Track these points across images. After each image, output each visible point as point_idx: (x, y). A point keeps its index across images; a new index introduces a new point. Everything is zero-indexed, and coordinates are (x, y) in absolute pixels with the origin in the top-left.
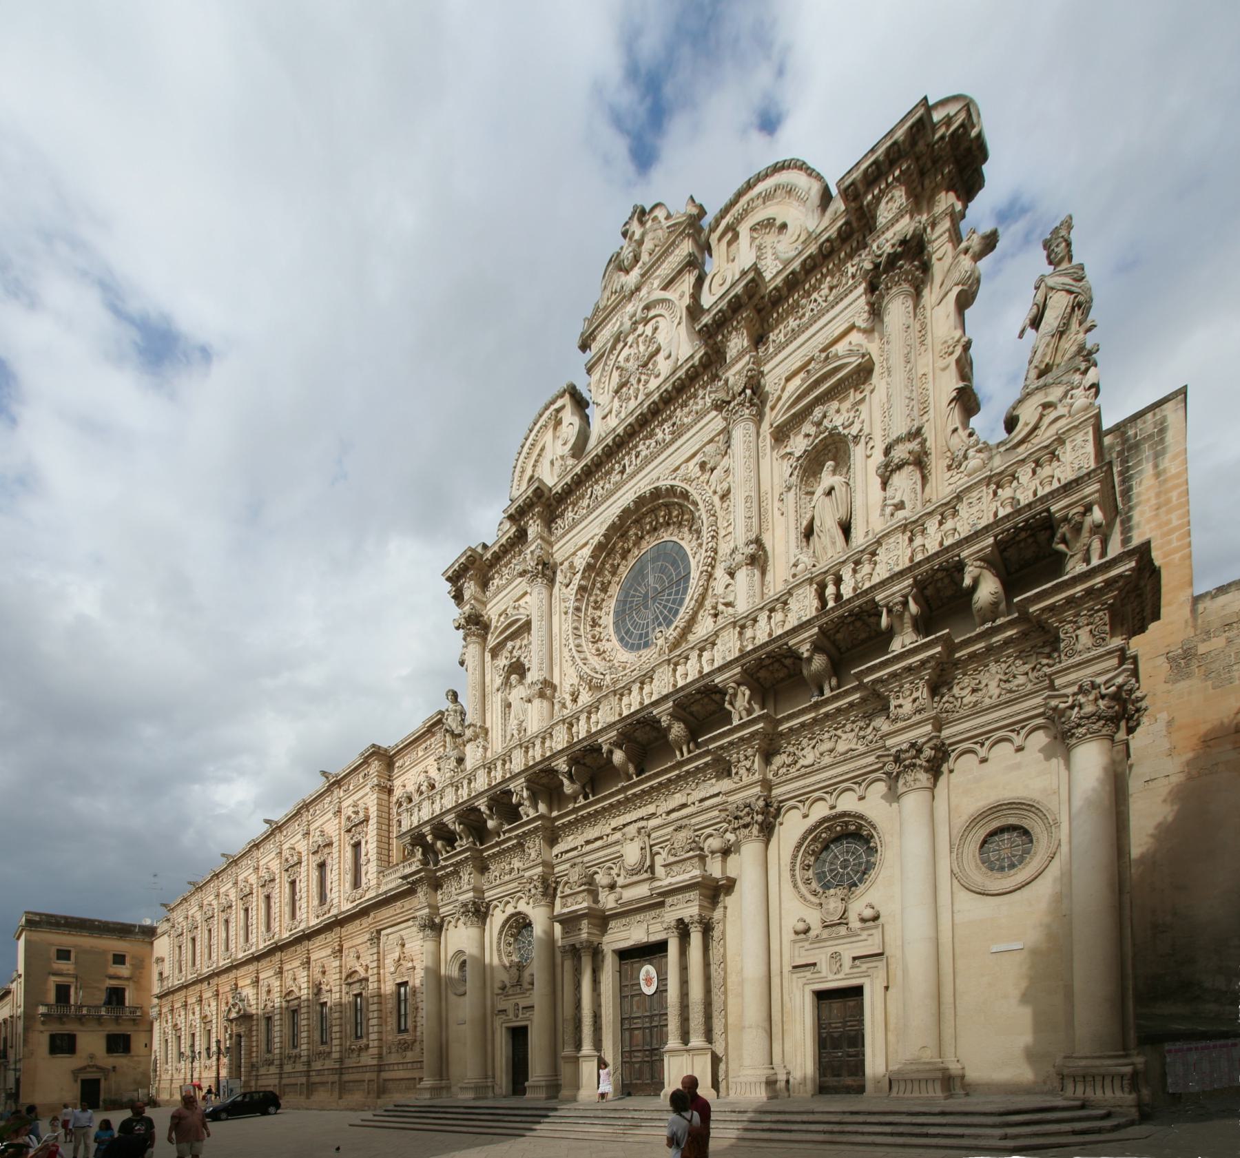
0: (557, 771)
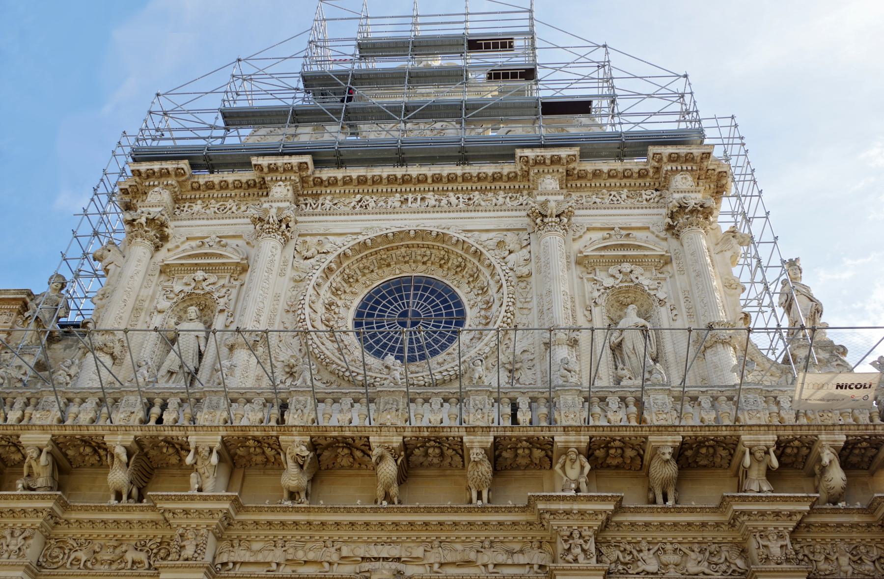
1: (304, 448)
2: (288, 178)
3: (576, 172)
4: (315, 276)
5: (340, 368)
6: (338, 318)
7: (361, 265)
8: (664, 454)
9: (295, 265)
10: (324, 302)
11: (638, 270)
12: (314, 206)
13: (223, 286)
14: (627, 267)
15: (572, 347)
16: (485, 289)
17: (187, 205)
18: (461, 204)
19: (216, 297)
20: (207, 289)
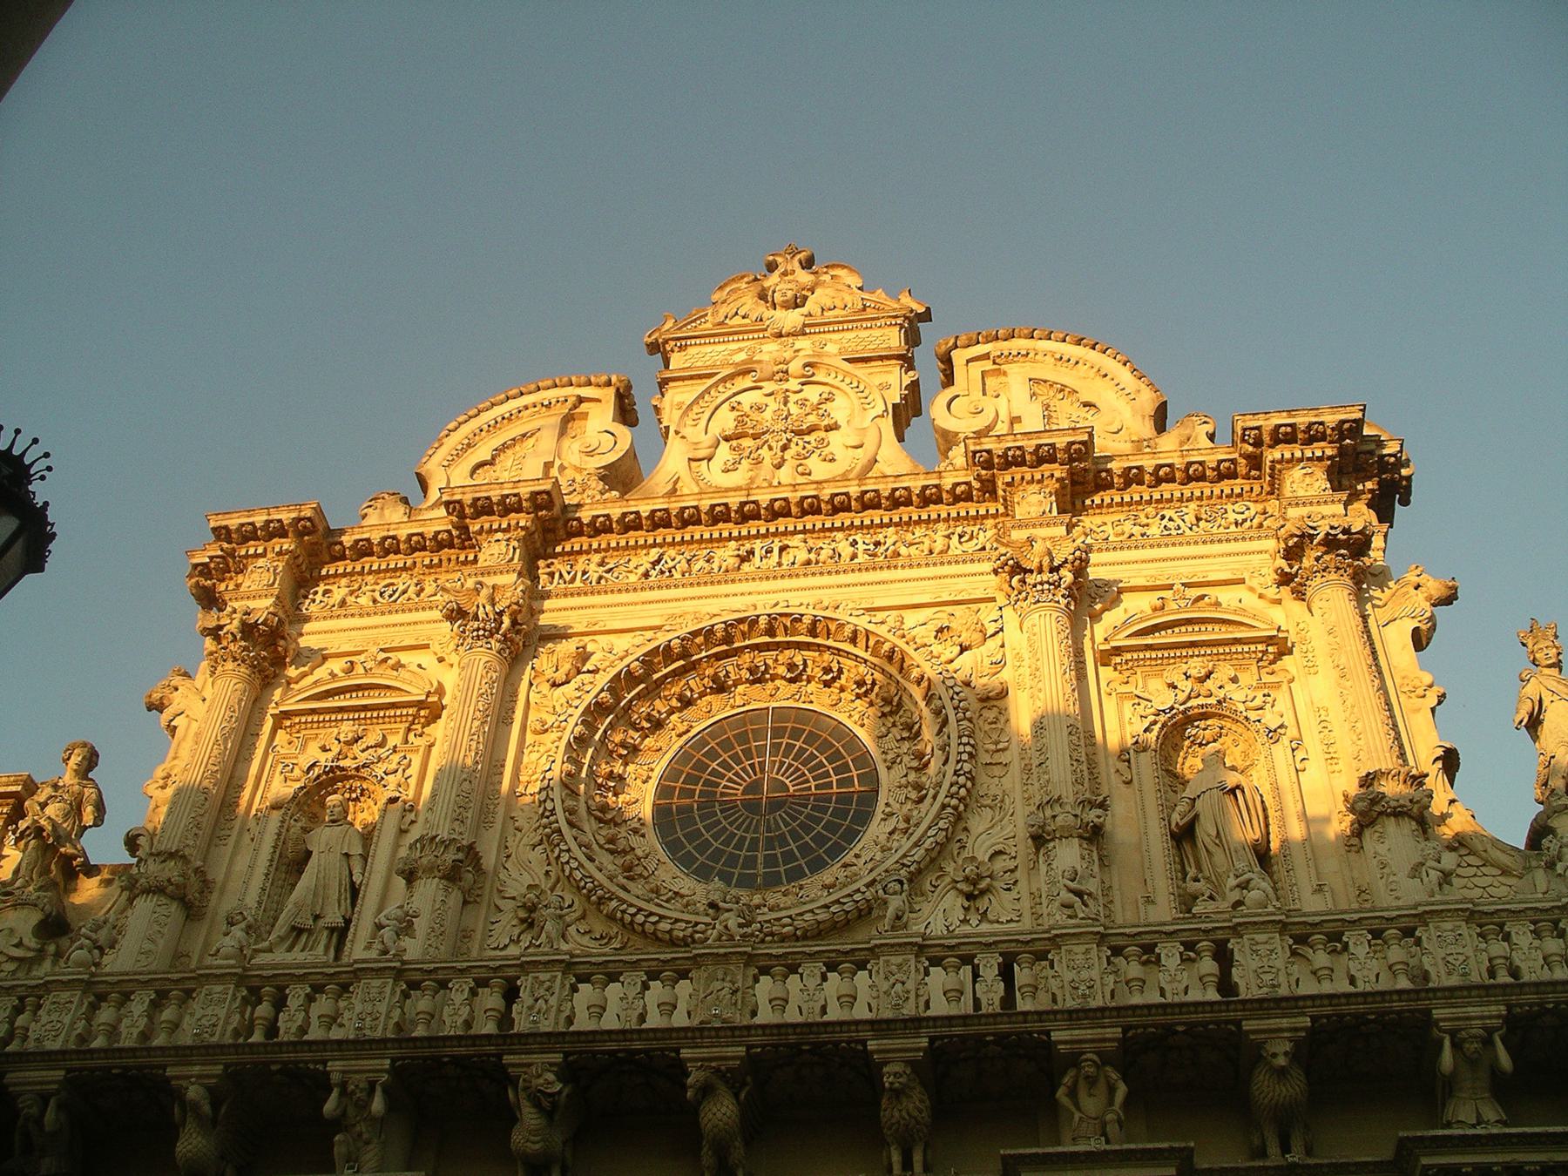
0: (513, 1082)
1: (551, 1077)
2: (513, 523)
3: (1091, 476)
8: (1274, 1055)
11: (1224, 671)
12: (568, 577)
14: (1196, 666)
15: (1090, 840)
16: (917, 727)
17: (321, 588)
18: (860, 554)
20: (363, 758)
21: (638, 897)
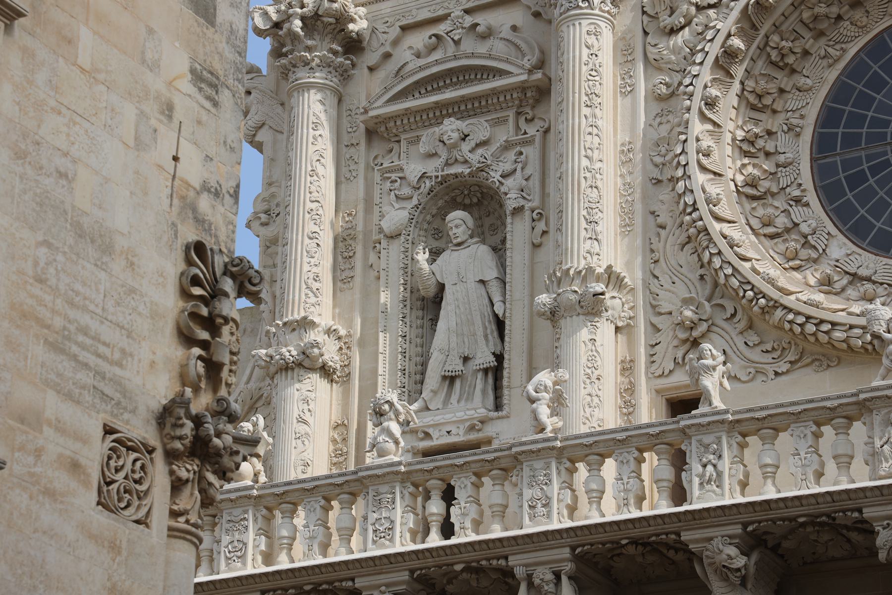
4: (699, 83)
5: (791, 316)
6: (778, 166)
7: (806, 15)
9: (651, 57)
10: (734, 139)
13: (507, 146)
19: (496, 176)
21: (805, 303)
